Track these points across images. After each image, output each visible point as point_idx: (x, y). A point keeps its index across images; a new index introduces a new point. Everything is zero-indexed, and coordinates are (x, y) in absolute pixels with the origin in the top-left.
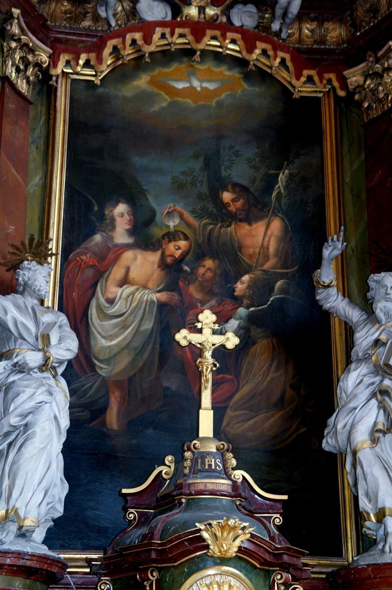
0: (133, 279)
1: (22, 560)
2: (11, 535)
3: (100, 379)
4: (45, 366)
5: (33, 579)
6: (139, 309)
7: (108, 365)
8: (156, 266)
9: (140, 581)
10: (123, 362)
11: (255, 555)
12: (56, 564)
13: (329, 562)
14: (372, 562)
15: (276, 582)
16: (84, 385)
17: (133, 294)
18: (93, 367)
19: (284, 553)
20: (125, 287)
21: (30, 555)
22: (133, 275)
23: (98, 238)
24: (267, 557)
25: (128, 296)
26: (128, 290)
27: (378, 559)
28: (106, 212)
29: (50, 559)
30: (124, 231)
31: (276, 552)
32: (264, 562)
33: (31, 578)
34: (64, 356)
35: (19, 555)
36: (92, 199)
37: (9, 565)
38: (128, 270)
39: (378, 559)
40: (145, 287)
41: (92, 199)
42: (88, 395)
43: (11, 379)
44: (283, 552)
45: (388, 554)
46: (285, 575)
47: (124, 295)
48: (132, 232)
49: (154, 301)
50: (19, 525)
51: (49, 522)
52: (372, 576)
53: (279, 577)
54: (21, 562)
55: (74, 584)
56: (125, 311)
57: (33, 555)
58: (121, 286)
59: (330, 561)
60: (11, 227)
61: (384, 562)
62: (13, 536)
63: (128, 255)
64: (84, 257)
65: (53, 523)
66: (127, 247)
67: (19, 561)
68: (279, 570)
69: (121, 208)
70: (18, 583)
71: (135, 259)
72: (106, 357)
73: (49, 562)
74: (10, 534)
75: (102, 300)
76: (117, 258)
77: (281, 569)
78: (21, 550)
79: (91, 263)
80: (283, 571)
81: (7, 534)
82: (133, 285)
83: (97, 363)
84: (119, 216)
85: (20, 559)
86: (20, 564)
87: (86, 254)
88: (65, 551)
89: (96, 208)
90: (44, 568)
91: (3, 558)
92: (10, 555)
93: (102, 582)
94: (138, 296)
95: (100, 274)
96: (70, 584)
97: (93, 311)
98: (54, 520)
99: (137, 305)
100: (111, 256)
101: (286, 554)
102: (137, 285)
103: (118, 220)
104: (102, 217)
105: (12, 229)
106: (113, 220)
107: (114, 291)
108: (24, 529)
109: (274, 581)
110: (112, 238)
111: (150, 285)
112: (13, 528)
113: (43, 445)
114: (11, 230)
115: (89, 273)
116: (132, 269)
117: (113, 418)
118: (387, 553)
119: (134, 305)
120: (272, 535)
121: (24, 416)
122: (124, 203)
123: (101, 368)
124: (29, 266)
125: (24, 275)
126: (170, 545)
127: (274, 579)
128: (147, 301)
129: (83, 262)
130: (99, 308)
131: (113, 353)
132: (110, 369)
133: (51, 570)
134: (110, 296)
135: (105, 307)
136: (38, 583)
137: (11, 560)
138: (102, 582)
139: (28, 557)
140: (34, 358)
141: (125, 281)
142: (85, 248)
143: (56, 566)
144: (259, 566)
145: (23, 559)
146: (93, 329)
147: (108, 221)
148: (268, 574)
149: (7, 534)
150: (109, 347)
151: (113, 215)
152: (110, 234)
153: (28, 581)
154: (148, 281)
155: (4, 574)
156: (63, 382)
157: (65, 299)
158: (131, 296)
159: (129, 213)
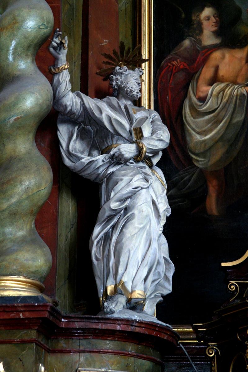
0: (223, 76)
1: (131, 327)
2: (119, 306)
3: (198, 170)
4: (140, 157)
5: (145, 346)
6: (229, 104)
7: (204, 157)
8: (244, 62)
9: (241, 340)
10: (218, 154)
16: (182, 178)
17: (223, 90)
18: (190, 160)
20: (215, 85)
21: (137, 322)
22: (222, 72)
23: (187, 43)
25: (219, 93)
26: (218, 87)
28: (193, 18)
30: (211, 33)
34: (156, 146)
35: (128, 322)
36: (179, 8)
37: (119, 331)
38: (217, 69)
40: (234, 83)
41: (179, 8)
42: (187, 186)
43: (111, 170)
47: (215, 93)
48: (217, 34)
49: (244, 95)
50: (127, 298)
51: (158, 297)
54: (130, 329)
56: (216, 107)
57: (141, 322)
58: (211, 83)
60: (105, 41)
62: (122, 306)
63: (217, 55)
64: (175, 63)
65: (162, 299)
66: (215, 48)
67: (128, 327)
69: (207, 12)
70: (130, 348)
71: (223, 57)
72: (202, 151)
73: (157, 329)
74: (119, 304)
75: (194, 99)
76: (206, 59)
78: (130, 318)
79: (181, 67)
81: (116, 305)
82: (222, 82)
83: (194, 156)
84: (206, 20)
85: (129, 326)
86: (130, 330)
87: (176, 60)
88: (178, 325)
89: (183, 16)
90: (153, 335)
91: (113, 325)
92: (119, 322)
93: (210, 347)
94: (228, 91)
95: (191, 76)
97: (187, 110)
98: (163, 296)
99: (228, 100)
100: (200, 57)
102: (226, 81)
103: (205, 23)
104: (189, 22)
105: (106, 42)
106: (200, 24)
107: (205, 89)
108: (133, 301)
110: (200, 42)
111: (239, 80)
112: (122, 300)
113: (142, 226)
114: (105, 44)
115: (181, 76)
116: (221, 67)
117: (212, 204)
119: (225, 100)
121: (122, 200)
122: (209, 7)
123: (198, 161)
124: (121, 71)
125: (117, 79)
128: (237, 95)
129: (174, 67)
130: (193, 108)
131: (208, 146)
132: (207, 161)
133: (160, 336)
134: (202, 95)
135: (197, 105)
136: (150, 349)
137: (121, 327)
138: (210, 347)
139: (136, 324)
140: (128, 150)
141: (214, 80)
142: (176, 54)
145: (132, 326)
146: (188, 126)
147: (195, 26)
149: (116, 305)
150: (204, 141)
151: (200, 19)
152: (198, 37)
153: (140, 347)
154: (237, 77)
155: (116, 339)
156: (159, 173)
157: (160, 102)
158: (222, 93)
159: (215, 16)
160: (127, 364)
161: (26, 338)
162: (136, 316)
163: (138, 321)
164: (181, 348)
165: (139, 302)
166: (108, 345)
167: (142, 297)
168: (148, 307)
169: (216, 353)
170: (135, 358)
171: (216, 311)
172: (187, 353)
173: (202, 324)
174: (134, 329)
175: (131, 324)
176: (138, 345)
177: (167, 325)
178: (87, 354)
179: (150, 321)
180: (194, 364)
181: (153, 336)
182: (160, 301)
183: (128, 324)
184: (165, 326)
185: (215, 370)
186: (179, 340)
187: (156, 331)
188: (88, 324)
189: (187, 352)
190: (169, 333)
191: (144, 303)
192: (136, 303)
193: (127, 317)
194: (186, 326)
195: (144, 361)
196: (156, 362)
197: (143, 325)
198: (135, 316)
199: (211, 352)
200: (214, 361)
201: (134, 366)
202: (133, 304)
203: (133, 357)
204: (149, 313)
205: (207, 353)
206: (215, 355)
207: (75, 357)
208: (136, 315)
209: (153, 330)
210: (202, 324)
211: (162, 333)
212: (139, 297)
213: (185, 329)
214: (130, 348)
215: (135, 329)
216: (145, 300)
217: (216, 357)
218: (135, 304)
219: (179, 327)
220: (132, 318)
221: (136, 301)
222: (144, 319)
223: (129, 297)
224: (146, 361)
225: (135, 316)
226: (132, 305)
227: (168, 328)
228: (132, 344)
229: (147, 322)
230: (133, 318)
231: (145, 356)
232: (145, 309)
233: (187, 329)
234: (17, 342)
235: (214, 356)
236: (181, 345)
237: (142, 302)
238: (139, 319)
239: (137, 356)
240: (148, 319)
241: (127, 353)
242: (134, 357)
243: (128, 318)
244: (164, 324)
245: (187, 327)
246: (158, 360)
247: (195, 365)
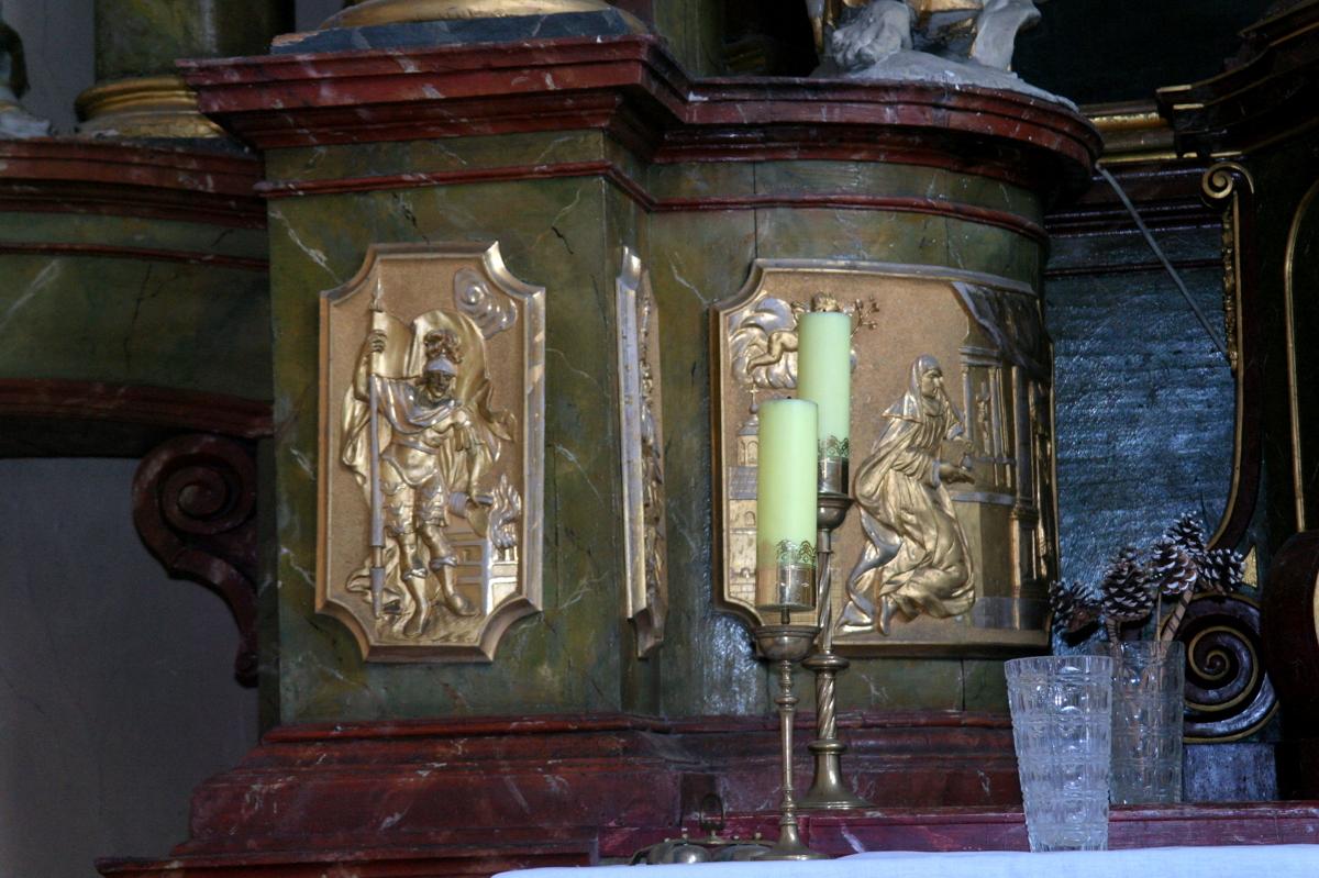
1: (934, 112)
2: (889, 38)
5: (983, 175)
12: (1052, 124)
21: (956, 93)
29: (1026, 106)
33: (973, 169)
35: (923, 94)
37: (892, 128)
50: (914, 10)
54: (930, 118)
55: (1134, 203)
57: (968, 94)
62: (897, 41)
67: (924, 113)
70: (932, 187)
73: (1026, 116)
74: (886, 33)
78: (927, 79)
81: (877, 37)
85: (926, 108)
86: (930, 124)
90: (1012, 135)
91: (871, 107)
92: (893, 97)
93: (1217, 166)
96: (1121, 204)
108: (936, 22)
136: (1001, 186)
137: (897, 112)
138: (1217, 166)
139: (953, 102)
143: (1053, 129)
145: (937, 107)
149: (877, 37)
153: (966, 181)
155: (882, 158)
160: (924, 240)
161: (572, 160)
162: (950, 74)
163: (957, 88)
164: (1106, 182)
165: (955, 24)
166: (853, 176)
167: (968, 6)
168: (986, 45)
169: (1240, 186)
170: (951, 221)
171: (1245, 30)
172: (1126, 200)
173: (1188, 87)
174: (943, 118)
175: (933, 101)
176: (958, 176)
177: (1062, 99)
178: (781, 211)
179: (1001, 87)
180: (1152, 234)
181: (1013, 140)
182: (1030, 20)
183: (924, 101)
184: (1051, 102)
185: (1233, 243)
186: (1100, 157)
187: (1023, 121)
188: (781, 106)
189: (1127, 195)
190: (1066, 129)
191: (973, 30)
192: (946, 29)
193: (919, 78)
194: (1119, 107)
195: (980, 228)
196: (1021, 231)
197: (975, 105)
198: (947, 72)
199: (1219, 183)
200: (1231, 213)
201: (948, 247)
202: (936, 32)
203: (943, 215)
204: (991, 59)
205: (1206, 186)
206: (1235, 193)
207: (742, 222)
208: (952, 71)
209: (1010, 117)
210: (1188, 87)
211: (1043, 130)
212: (958, 7)
213: (1118, 118)
214: (933, 185)
215: (949, 116)
216: (977, 14)
217: (1236, 198)
218: (942, 35)
219: (1096, 113)
220: (936, 80)
221: (947, 23)
222: (978, 83)
223: (922, 8)
224: (987, 227)
225: (947, 72)
226: (933, 33)
227: (1065, 111)
228: (938, 170)
229: (989, 93)
230: (940, 80)
231: (982, 211)
232: (977, 49)
233: (1126, 118)
234: (541, 176)
235: (1230, 196)
236: (1106, 173)
237: (969, 22)
238: (961, 83)
239: (957, 211)
240: (995, 82)
241: (923, 203)
242: (946, 216)
243: (922, 80)
244: (1052, 97)
245: (1125, 110)
246: (1030, 223)
247: (1157, 237)
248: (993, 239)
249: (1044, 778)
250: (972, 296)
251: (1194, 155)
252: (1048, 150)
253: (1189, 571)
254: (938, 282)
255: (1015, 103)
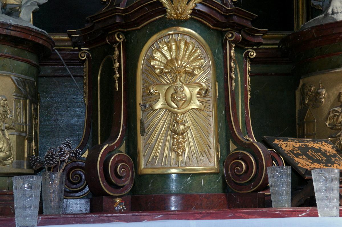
1: (6, 30)
9: (110, 44)
11: (209, 18)
12: (40, 37)
13: (282, 35)
14: (316, 25)
15: (228, 40)
19: (234, 15)
24: (219, 18)
27: (321, 21)
29: (33, 31)
31: (227, 14)
32: (217, 23)
33: (18, 47)
39: (321, 21)
44: (233, 13)
45: (330, 16)
46: (235, 34)
51: (34, 5)
52: (316, 36)
53: (230, 35)
55: (64, 59)
57: (16, 27)
59: (283, 34)
61: (326, 22)
65: (38, 7)
67: (4, 31)
68: (230, 30)
73: (32, 34)
77: (232, 30)
78: (5, 21)
80: (234, 32)
85: (4, 29)
86: (5, 33)
88: (54, 33)
93: (82, 51)
96: (60, 59)
98: (39, 5)
101: (236, 15)
108: (8, 7)
109: (226, 39)
118: (329, 15)
120: (225, 2)
126: (133, 11)
127: (226, 37)
133: (35, 41)
136: (26, 52)
138: (82, 51)
139: (12, 28)
143: (40, 38)
144: (212, 27)
145: (8, 29)
148: (221, 34)
153: (16, 50)
160: (3, 64)
162: (11, 21)
163: (13, 25)
164: (56, 53)
165: (14, 8)
167: (17, 3)
168: (24, 14)
169: (88, 57)
170: (11, 60)
171: (88, 17)
172: (61, 58)
173: (75, 31)
174: (9, 32)
175: (6, 27)
176: (14, 48)
177: (43, 30)
179: (26, 26)
180: (68, 68)
181: (29, 40)
182: (36, 9)
183: (3, 27)
184: (40, 31)
185: (86, 71)
186: (54, 47)
187: (32, 35)
189: (62, 57)
190: (44, 38)
191: (20, 10)
192: (12, 9)
193: (2, 21)
194: (62, 34)
195: (20, 62)
196: (32, 64)
197: (18, 30)
198: (10, 20)
199: (83, 56)
200: (86, 64)
201: (10, 67)
202: (9, 9)
203: (9, 58)
204: (26, 18)
205: (79, 56)
206: (87, 58)
208: (12, 20)
209: (28, 34)
210: (75, 31)
211: (37, 38)
212: (14, 3)
213: (61, 37)
215: (11, 32)
216: (20, 6)
217: (87, 60)
218: (10, 10)
219: (55, 35)
220: (7, 22)
221: (12, 7)
222: (19, 24)
223: (4, 3)
224: (22, 62)
225: (10, 20)
226: (8, 10)
227: (43, 34)
228: (8, 46)
229: (22, 27)
230: (8, 22)
231: (20, 58)
232: (21, 15)
233: (63, 37)
235: (86, 59)
236: (56, 50)
237: (18, 8)
238: (14, 24)
239: (13, 57)
240: (24, 24)
241: (3, 54)
242: (10, 59)
243: (3, 22)
244: (40, 30)
245: (62, 35)
246: (34, 62)
247: (69, 69)
248: (23, 65)
249: (21, 208)
250: (16, 80)
251: (77, 48)
252: (38, 44)
253: (67, 154)
254: (7, 76)
255: (29, 30)
